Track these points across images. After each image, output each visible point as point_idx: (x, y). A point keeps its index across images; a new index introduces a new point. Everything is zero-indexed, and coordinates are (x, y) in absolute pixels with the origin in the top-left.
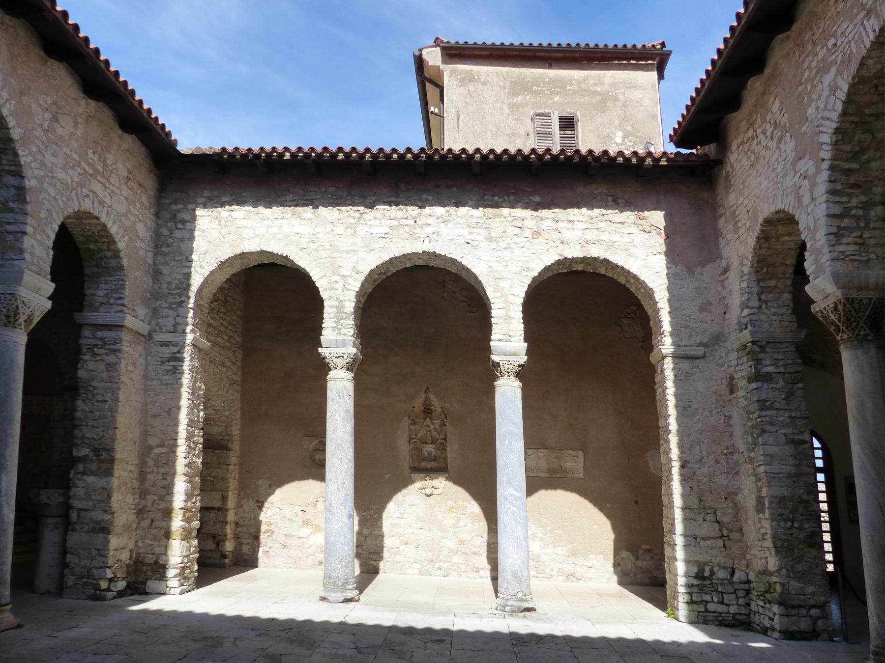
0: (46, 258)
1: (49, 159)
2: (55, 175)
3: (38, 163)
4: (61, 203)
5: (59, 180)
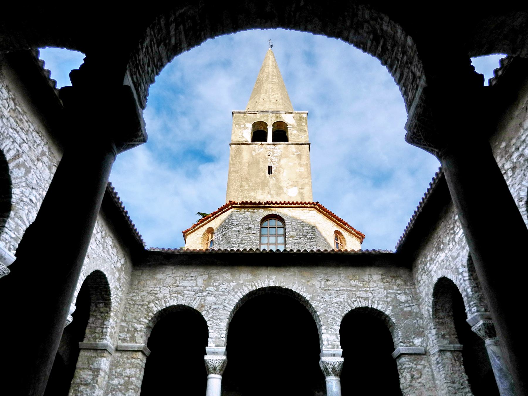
0: (336, 339)
2: (333, 302)
3: (323, 303)
4: (339, 312)
5: (336, 303)
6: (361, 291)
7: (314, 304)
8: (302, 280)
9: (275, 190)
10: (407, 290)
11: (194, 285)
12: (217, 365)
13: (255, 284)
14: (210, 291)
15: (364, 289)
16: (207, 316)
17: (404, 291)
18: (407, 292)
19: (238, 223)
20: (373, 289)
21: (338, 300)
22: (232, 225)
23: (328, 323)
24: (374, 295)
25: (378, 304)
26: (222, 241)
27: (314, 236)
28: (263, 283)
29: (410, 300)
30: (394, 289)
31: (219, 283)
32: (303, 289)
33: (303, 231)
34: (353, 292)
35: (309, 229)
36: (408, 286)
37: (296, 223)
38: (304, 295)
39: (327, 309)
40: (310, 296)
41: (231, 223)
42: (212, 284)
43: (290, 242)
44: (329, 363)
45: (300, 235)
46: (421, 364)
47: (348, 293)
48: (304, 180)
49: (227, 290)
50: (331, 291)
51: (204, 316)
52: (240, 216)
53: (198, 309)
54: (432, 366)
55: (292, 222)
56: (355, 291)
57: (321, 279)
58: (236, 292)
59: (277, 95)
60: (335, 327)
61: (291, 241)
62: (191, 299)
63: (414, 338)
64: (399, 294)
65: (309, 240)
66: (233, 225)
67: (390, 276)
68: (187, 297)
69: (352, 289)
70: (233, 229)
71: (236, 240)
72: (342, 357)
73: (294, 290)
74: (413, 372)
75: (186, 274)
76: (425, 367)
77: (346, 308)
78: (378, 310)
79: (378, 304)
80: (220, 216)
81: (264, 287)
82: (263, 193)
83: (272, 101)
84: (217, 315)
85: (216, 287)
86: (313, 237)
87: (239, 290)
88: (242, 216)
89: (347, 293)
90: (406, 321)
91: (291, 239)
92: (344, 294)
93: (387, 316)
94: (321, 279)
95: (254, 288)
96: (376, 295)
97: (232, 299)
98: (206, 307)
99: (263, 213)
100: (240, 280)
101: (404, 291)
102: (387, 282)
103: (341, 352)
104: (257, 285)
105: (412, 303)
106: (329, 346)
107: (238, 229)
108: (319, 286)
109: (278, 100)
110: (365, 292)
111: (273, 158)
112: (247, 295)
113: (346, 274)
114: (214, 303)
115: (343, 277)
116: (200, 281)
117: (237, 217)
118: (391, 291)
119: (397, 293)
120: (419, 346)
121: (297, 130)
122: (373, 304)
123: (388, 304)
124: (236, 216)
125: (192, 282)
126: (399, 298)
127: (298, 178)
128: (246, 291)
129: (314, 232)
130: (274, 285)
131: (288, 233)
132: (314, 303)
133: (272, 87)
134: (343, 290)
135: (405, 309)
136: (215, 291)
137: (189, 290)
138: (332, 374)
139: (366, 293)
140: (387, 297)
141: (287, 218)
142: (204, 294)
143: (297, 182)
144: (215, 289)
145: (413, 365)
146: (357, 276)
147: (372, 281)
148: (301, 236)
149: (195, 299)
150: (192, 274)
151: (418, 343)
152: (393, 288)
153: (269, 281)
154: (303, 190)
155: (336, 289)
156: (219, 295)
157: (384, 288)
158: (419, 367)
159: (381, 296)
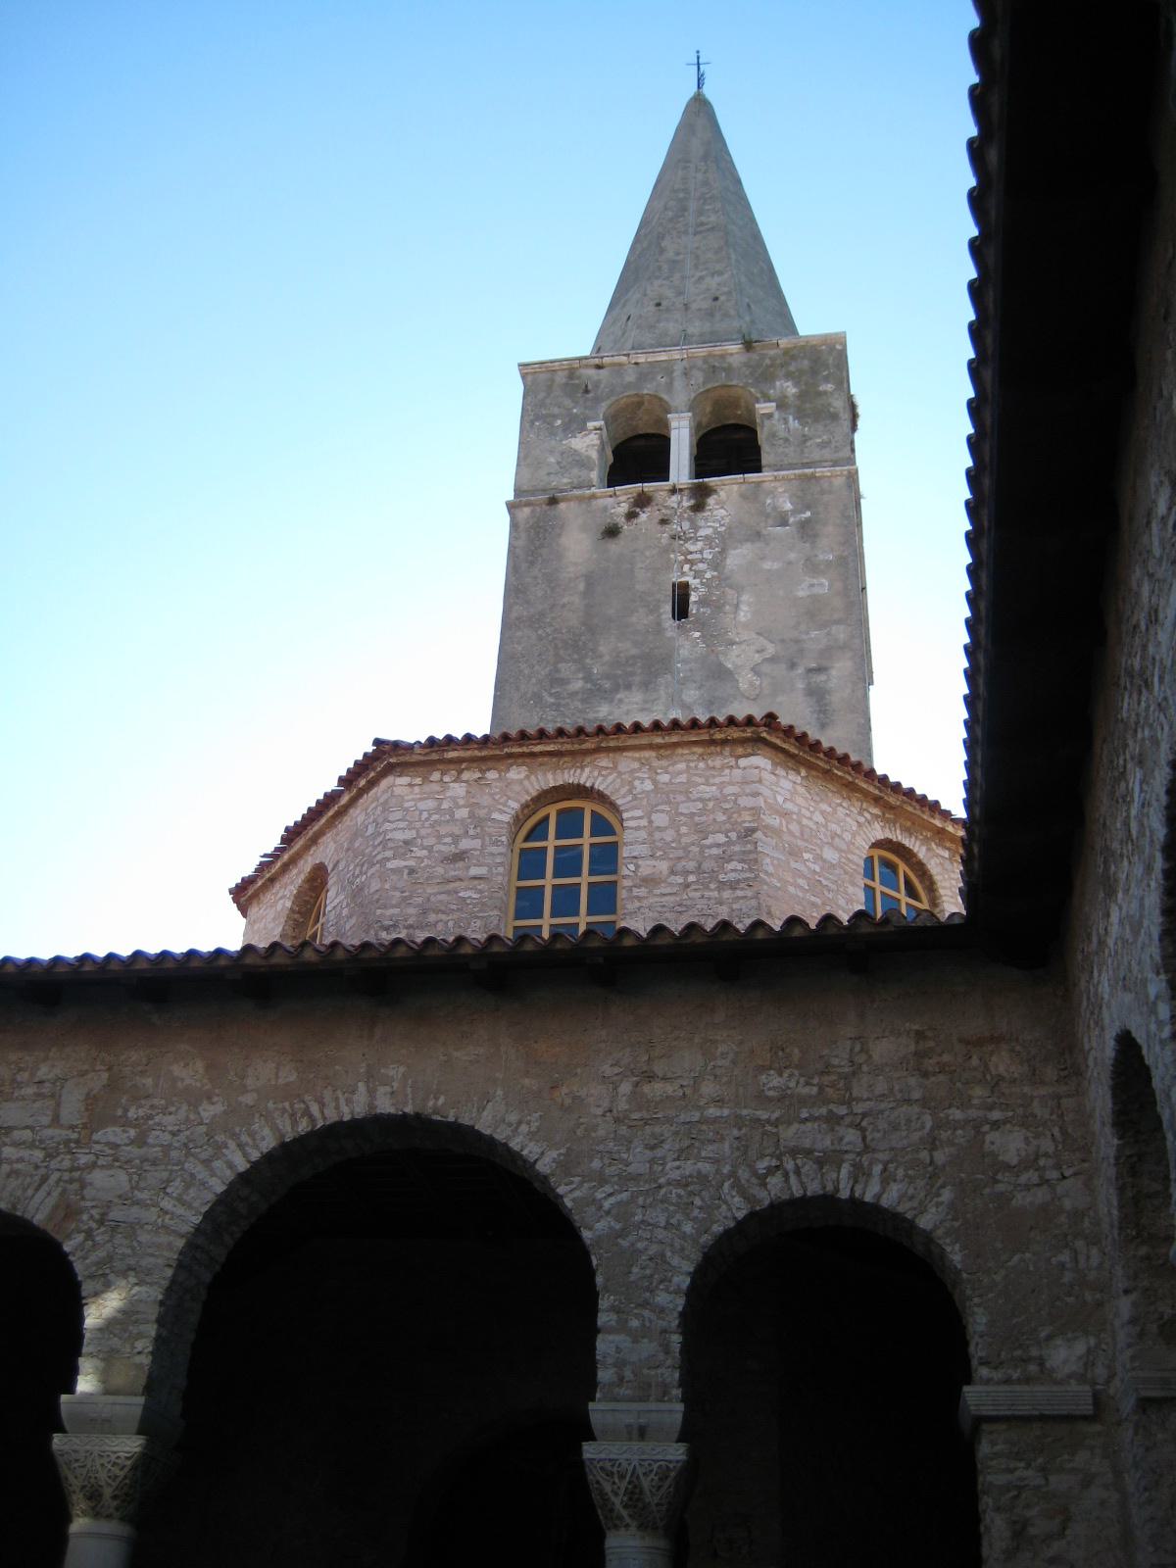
0: (661, 1356)
1: (638, 1160)
2: (662, 1180)
4: (688, 1228)
5: (678, 1184)
6: (806, 1119)
7: (570, 1193)
8: (527, 1081)
9: (700, 688)
10: (1036, 1103)
11: (46, 1120)
12: (103, 1476)
13: (308, 1107)
14: (107, 1143)
15: (824, 1111)
16: (85, 1258)
17: (1020, 1111)
18: (1038, 1111)
19: (409, 835)
20: (868, 1105)
21: (689, 1168)
22: (385, 849)
23: (632, 1278)
24: (869, 1138)
25: (887, 1179)
26: (350, 916)
27: (751, 870)
28: (342, 1102)
29: (1046, 1155)
30: (975, 1102)
31: (152, 1107)
32: (529, 1123)
33: (702, 852)
34: (768, 1128)
35: (729, 843)
36: (1042, 1083)
37: (672, 821)
38: (531, 1151)
39: (634, 1215)
40: (554, 1154)
41: (380, 839)
42: (119, 1112)
43: (637, 904)
44: (615, 1469)
45: (686, 873)
46: (1071, 1465)
47: (744, 1131)
48: (828, 634)
49: (182, 1137)
50: (657, 1129)
51: (71, 1258)
52: (422, 805)
53: (50, 1229)
54: (1126, 1475)
55: (654, 817)
56: (776, 1123)
57: (617, 1070)
58: (220, 1147)
59: (717, 279)
60: (662, 1298)
61: (645, 903)
62: (28, 1180)
63: (1049, 1338)
64: (996, 1125)
65: (727, 894)
66: (390, 844)
67: (961, 1040)
68: (8, 1176)
69: (764, 1115)
70: (390, 865)
71: (396, 911)
72: (677, 1442)
73: (485, 1124)
74: (1028, 1506)
75: (20, 1070)
76: (1087, 1482)
77: (724, 1207)
78: (886, 1210)
79: (887, 1179)
80: (351, 811)
81: (347, 1118)
82: (646, 702)
83: (694, 306)
84: (129, 1251)
85: (135, 1127)
86: (748, 875)
87: (235, 1136)
88: (430, 804)
89: (735, 1132)
90: (1016, 1258)
91: (642, 892)
92: (722, 1139)
93: (928, 1237)
94: (617, 1070)
95: (304, 1127)
96: (878, 1135)
97: (200, 1177)
98: (85, 1217)
99: (526, 783)
100: (244, 1090)
101: (1020, 1111)
102: (942, 1069)
103: (679, 1418)
104: (315, 1109)
105: (1058, 1166)
106: (624, 1391)
107: (411, 863)
108: (606, 1104)
109: (722, 298)
110: (824, 1126)
111: (692, 548)
112: (269, 1158)
113: (741, 1043)
114: (120, 1197)
115: (724, 1055)
116: (72, 1106)
117: (407, 810)
118: (956, 1114)
119: (986, 1121)
120: (1070, 1376)
121: (801, 415)
122: (862, 1179)
123: (933, 1176)
124: (406, 805)
125: (37, 1105)
126: (992, 1147)
127: (803, 627)
128: (263, 1139)
129: (752, 856)
130: (392, 1111)
131: (632, 867)
132: (569, 1188)
133: (697, 248)
134: (716, 1120)
135: (1020, 1200)
136: (132, 1142)
137: (24, 1143)
138: (628, 1520)
139: (833, 1130)
140: (933, 1143)
141: (629, 798)
142: (83, 1160)
143: (797, 641)
144: (132, 1133)
145: (1030, 1473)
146: (796, 1051)
147: (865, 1068)
148: (692, 878)
149: (44, 1179)
150: (43, 1072)
151: (1065, 1362)
152: (970, 1098)
153: (371, 1093)
154: (823, 678)
155: (683, 1117)
156: (147, 1160)
157: (924, 1102)
158: (1058, 1482)
159: (905, 1142)
